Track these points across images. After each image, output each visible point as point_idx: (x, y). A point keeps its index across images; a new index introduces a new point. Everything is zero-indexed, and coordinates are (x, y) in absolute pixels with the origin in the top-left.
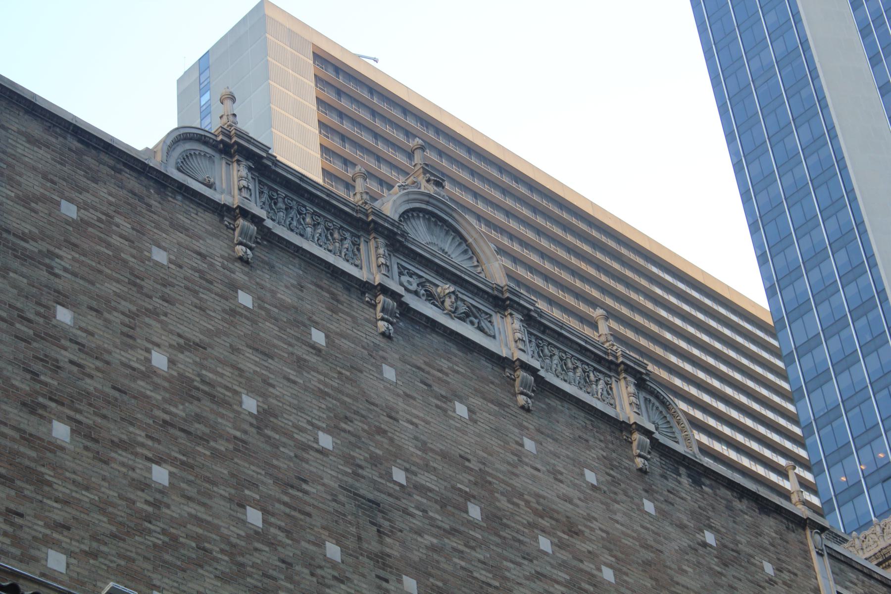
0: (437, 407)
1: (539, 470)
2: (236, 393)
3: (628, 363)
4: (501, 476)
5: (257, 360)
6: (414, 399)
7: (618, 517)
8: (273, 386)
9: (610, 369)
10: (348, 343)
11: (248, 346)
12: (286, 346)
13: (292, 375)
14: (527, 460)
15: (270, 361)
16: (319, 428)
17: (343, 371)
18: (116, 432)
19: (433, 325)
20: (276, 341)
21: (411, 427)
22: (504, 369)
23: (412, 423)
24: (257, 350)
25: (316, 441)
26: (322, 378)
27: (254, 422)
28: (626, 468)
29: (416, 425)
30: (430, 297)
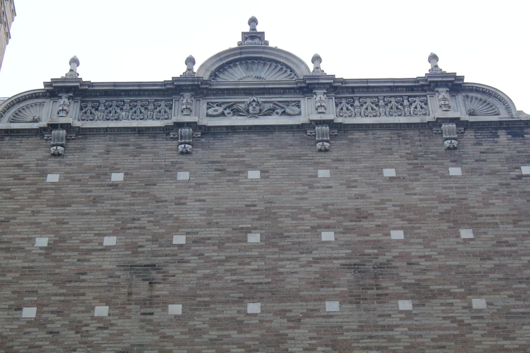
0: (228, 181)
1: (331, 187)
2: (31, 239)
3: (436, 79)
4: (288, 205)
5: (55, 211)
6: (206, 184)
7: (418, 190)
8: (67, 223)
9: (425, 91)
10: (145, 171)
11: (48, 206)
12: (84, 194)
13: (86, 209)
14: (319, 185)
15: (67, 208)
16: (105, 235)
17: (137, 191)
19: (233, 130)
20: (75, 194)
21: (198, 203)
22: (306, 132)
23: (200, 201)
24: (57, 206)
25: (101, 244)
26: (116, 202)
27: (43, 252)
28: (432, 153)
29: (204, 201)
30: (236, 112)
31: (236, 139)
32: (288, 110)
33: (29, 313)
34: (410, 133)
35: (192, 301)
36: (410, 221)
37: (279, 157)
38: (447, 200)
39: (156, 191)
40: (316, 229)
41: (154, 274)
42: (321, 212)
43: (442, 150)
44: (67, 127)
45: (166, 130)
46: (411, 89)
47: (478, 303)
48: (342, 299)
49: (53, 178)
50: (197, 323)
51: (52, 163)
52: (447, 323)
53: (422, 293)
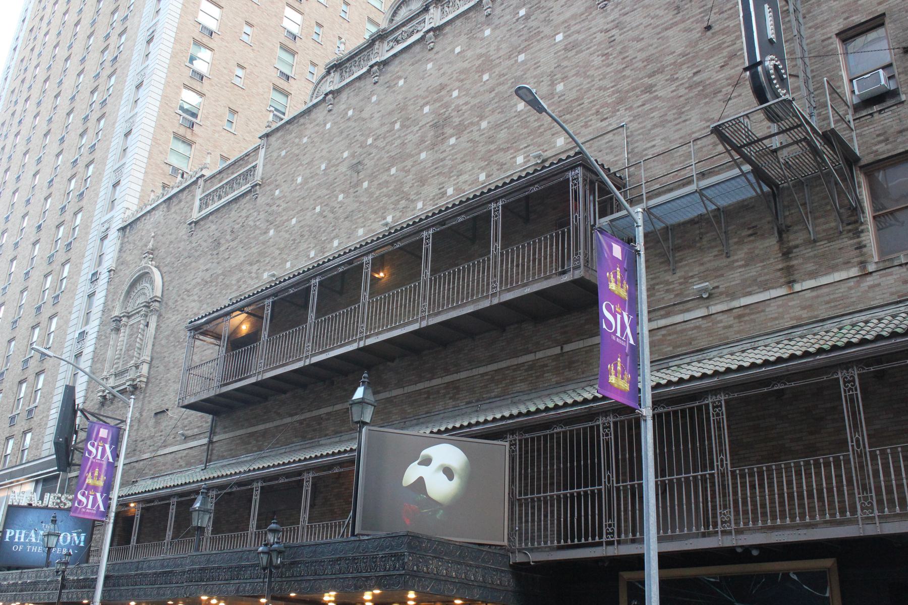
18: (285, 218)
19: (395, 56)
31: (397, 61)
32: (419, 29)
33: (318, 209)
34: (471, 14)
35: (372, 177)
36: (462, 81)
37: (413, 64)
38: (480, 56)
40: (422, 107)
41: (360, 167)
42: (426, 93)
43: (484, 19)
44: (331, 92)
45: (369, 71)
47: (484, 124)
48: (427, 149)
49: (328, 126)
50: (372, 190)
51: (329, 117)
52: (469, 145)
53: (460, 130)
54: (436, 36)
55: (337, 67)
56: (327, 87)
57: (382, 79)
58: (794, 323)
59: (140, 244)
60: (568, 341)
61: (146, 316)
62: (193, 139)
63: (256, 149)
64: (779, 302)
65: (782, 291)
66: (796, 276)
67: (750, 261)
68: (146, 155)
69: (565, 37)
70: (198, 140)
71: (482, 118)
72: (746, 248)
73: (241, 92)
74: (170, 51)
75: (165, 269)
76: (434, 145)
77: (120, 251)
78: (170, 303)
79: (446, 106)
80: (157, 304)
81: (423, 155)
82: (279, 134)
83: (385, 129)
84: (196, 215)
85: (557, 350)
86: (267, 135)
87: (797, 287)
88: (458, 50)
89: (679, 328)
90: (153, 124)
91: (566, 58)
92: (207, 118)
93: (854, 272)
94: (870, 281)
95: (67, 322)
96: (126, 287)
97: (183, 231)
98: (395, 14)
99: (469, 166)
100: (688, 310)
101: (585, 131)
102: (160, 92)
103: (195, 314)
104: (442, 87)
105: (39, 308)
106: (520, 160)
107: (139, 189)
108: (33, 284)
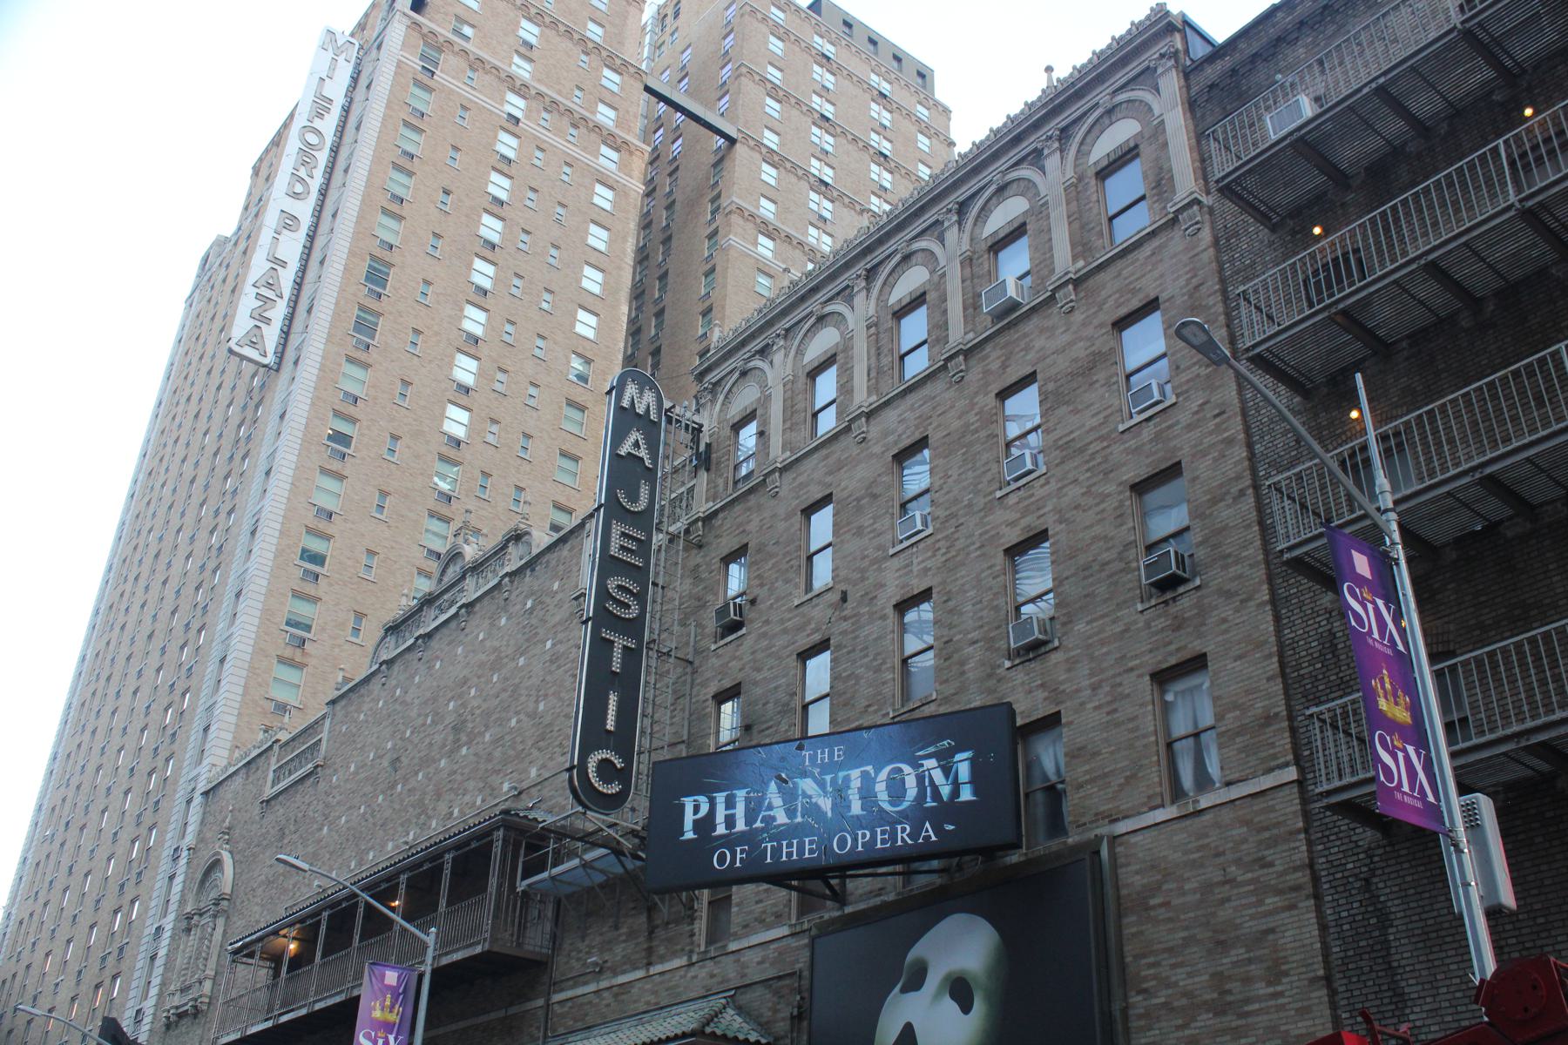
19: (437, 629)
39: (408, 699)
46: (496, 553)
54: (468, 613)
55: (394, 629)
56: (385, 656)
57: (427, 655)
58: (645, 1008)
59: (220, 818)
60: (511, 1004)
61: (215, 916)
62: (305, 661)
63: (324, 717)
64: (639, 985)
65: (640, 974)
66: (654, 958)
67: (632, 935)
68: (240, 690)
69: (554, 645)
70: (312, 662)
71: (487, 727)
72: (630, 921)
73: (371, 586)
74: (273, 549)
75: (238, 857)
76: (452, 751)
77: (203, 822)
78: (238, 902)
79: (464, 705)
80: (225, 903)
81: (443, 763)
82: (343, 703)
83: (420, 721)
84: (269, 792)
85: (502, 1013)
86: (333, 702)
87: (652, 971)
88: (481, 637)
89: (581, 1000)
90: (250, 649)
91: (550, 672)
92: (323, 629)
93: (683, 961)
94: (693, 971)
95: (147, 910)
96: (199, 876)
97: (257, 810)
98: (444, 572)
99: (471, 785)
100: (585, 983)
101: (551, 764)
102: (260, 606)
103: (258, 922)
104: (465, 681)
105: (122, 886)
106: (506, 786)
107: (229, 736)
108: (120, 850)
